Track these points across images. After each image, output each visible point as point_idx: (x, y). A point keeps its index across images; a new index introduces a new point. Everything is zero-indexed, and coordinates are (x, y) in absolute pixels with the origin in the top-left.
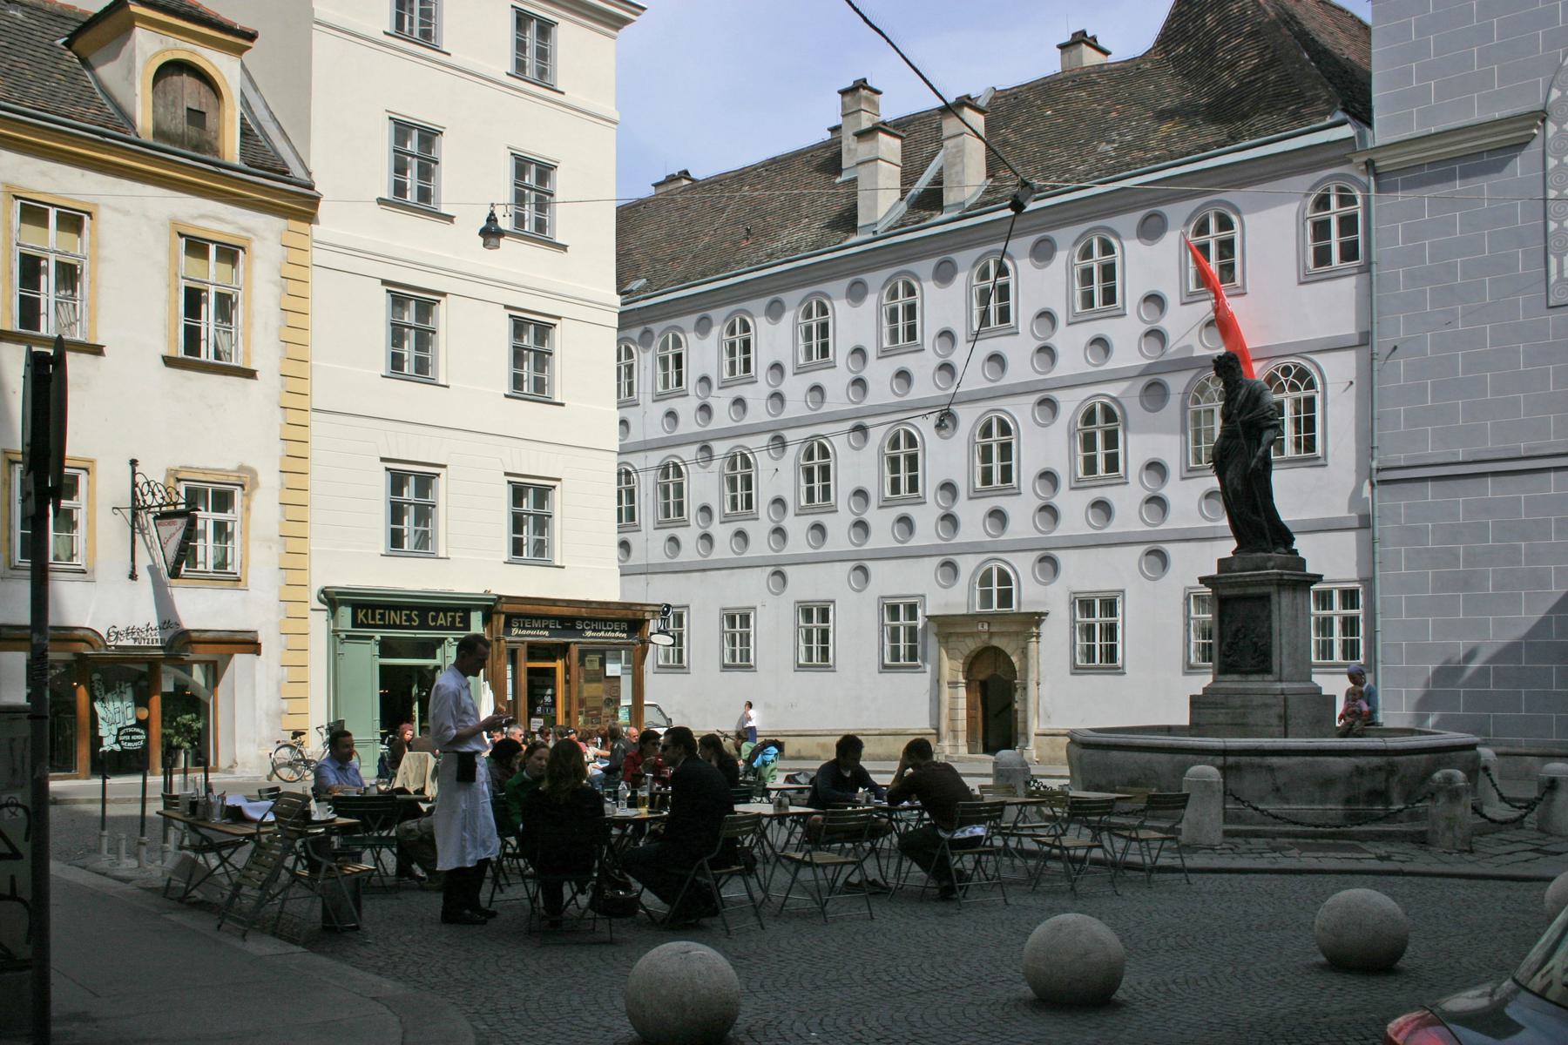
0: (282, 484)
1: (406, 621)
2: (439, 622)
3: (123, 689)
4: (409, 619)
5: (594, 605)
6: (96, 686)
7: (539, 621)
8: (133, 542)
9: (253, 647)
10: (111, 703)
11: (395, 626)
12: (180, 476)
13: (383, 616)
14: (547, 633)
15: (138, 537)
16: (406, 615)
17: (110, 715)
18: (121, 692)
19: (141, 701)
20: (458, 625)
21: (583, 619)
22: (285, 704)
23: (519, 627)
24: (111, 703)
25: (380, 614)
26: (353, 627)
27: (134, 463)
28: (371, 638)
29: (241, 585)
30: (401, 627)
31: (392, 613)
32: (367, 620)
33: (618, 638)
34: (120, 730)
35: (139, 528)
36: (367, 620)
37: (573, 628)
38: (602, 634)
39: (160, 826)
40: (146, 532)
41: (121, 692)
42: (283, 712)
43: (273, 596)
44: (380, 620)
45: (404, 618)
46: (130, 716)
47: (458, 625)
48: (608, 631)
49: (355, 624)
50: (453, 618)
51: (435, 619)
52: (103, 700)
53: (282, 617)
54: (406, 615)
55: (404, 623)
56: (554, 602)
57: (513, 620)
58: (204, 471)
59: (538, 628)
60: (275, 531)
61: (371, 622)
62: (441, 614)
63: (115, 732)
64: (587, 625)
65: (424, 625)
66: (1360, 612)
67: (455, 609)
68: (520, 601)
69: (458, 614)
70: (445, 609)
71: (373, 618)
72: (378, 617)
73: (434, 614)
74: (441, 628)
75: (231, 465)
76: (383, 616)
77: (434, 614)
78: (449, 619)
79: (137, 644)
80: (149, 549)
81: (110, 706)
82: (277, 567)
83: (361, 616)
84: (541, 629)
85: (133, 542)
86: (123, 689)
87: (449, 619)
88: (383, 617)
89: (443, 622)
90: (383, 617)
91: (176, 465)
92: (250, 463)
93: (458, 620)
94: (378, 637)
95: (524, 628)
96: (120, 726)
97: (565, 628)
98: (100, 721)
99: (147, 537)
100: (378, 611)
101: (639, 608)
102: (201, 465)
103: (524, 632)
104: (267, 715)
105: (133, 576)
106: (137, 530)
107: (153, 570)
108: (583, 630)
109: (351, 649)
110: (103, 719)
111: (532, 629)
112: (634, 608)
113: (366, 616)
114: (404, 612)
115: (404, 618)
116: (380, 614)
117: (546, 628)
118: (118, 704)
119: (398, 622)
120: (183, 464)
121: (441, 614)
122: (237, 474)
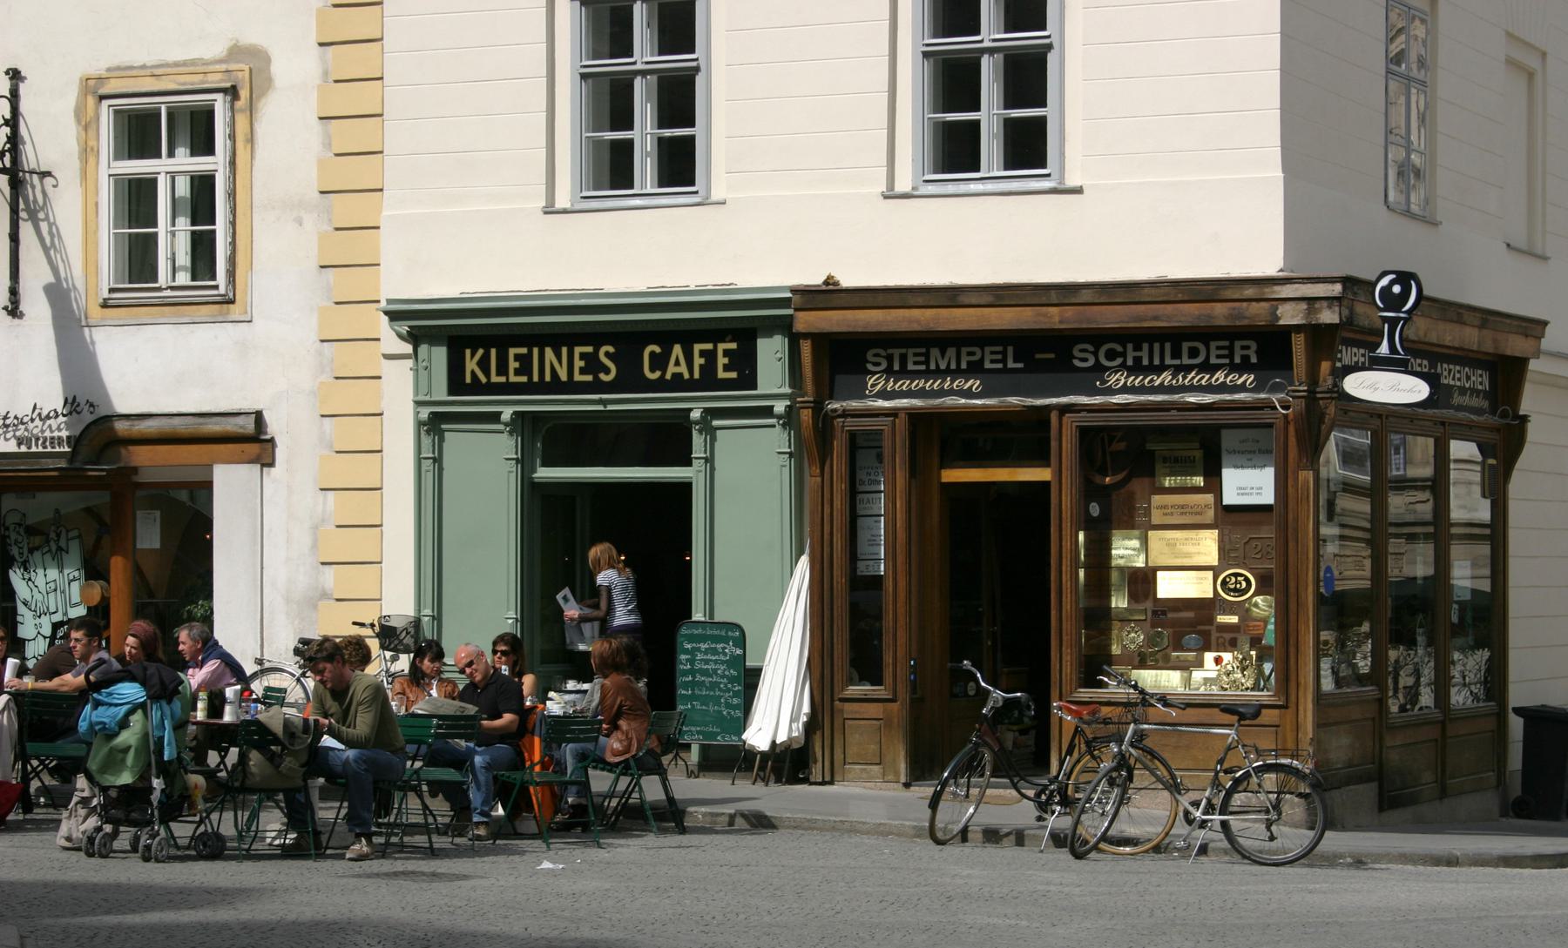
0: (326, 73)
1: (583, 371)
2: (672, 369)
3: (63, 543)
4: (592, 365)
5: (1086, 296)
6: (13, 536)
7: (951, 352)
8: (14, 238)
9: (253, 448)
10: (40, 572)
11: (556, 386)
12: (103, 91)
13: (525, 362)
14: (974, 384)
15: (26, 230)
16: (583, 356)
17: (38, 597)
18: (60, 549)
19: (94, 571)
20: (721, 374)
21: (1097, 338)
22: (329, 576)
23: (889, 372)
24: (40, 572)
25: (517, 357)
26: (451, 392)
27: (15, 75)
28: (495, 417)
29: (235, 311)
30: (572, 387)
31: (549, 353)
32: (487, 373)
33: (1223, 388)
34: (56, 626)
35: (28, 209)
36: (487, 373)
37: (1063, 363)
38: (1166, 378)
39: (367, 832)
40: (41, 215)
41: (60, 549)
42: (325, 595)
43: (306, 332)
44: (518, 372)
45: (578, 364)
46: (76, 598)
47: (721, 374)
48: (1187, 369)
49: (457, 383)
50: (710, 356)
51: (659, 362)
52: (25, 566)
53: (327, 378)
54: (583, 356)
55: (578, 377)
56: (950, 296)
57: (870, 356)
58: (154, 71)
59: (948, 371)
60: (307, 180)
61: (495, 379)
62: (677, 350)
63: (47, 631)
64: (1111, 355)
65: (630, 380)
66: (215, 163)
67: (714, 333)
68: (881, 299)
69: (721, 347)
70: (687, 335)
71: (503, 369)
72: (513, 365)
73: (657, 349)
74: (678, 384)
75: (212, 49)
76: (525, 362)
77: (657, 349)
78: (698, 361)
79: (24, 449)
80: (46, 250)
81: (40, 578)
82: (313, 264)
83: (471, 365)
84: (957, 373)
85: (14, 238)
86: (63, 543)
87: (698, 361)
88: (525, 365)
89: (683, 369)
90: (525, 365)
91: (98, 67)
92: (250, 38)
93: (722, 361)
94: (507, 413)
95: (904, 373)
96: (57, 618)
97: (1033, 367)
98: (21, 609)
99: (44, 226)
100: (512, 351)
101: (1250, 292)
102: (149, 60)
103: (904, 384)
104: (288, 601)
105: (14, 311)
106: (23, 215)
107: (58, 294)
108: (1099, 369)
109: (457, 441)
110: (25, 603)
111: (927, 374)
112: (1229, 293)
113: (484, 364)
114: (578, 350)
115: (578, 364)
116: (517, 357)
117: (975, 369)
118: (53, 573)
119: (563, 376)
120: (115, 62)
121: (677, 350)
122: (223, 67)
